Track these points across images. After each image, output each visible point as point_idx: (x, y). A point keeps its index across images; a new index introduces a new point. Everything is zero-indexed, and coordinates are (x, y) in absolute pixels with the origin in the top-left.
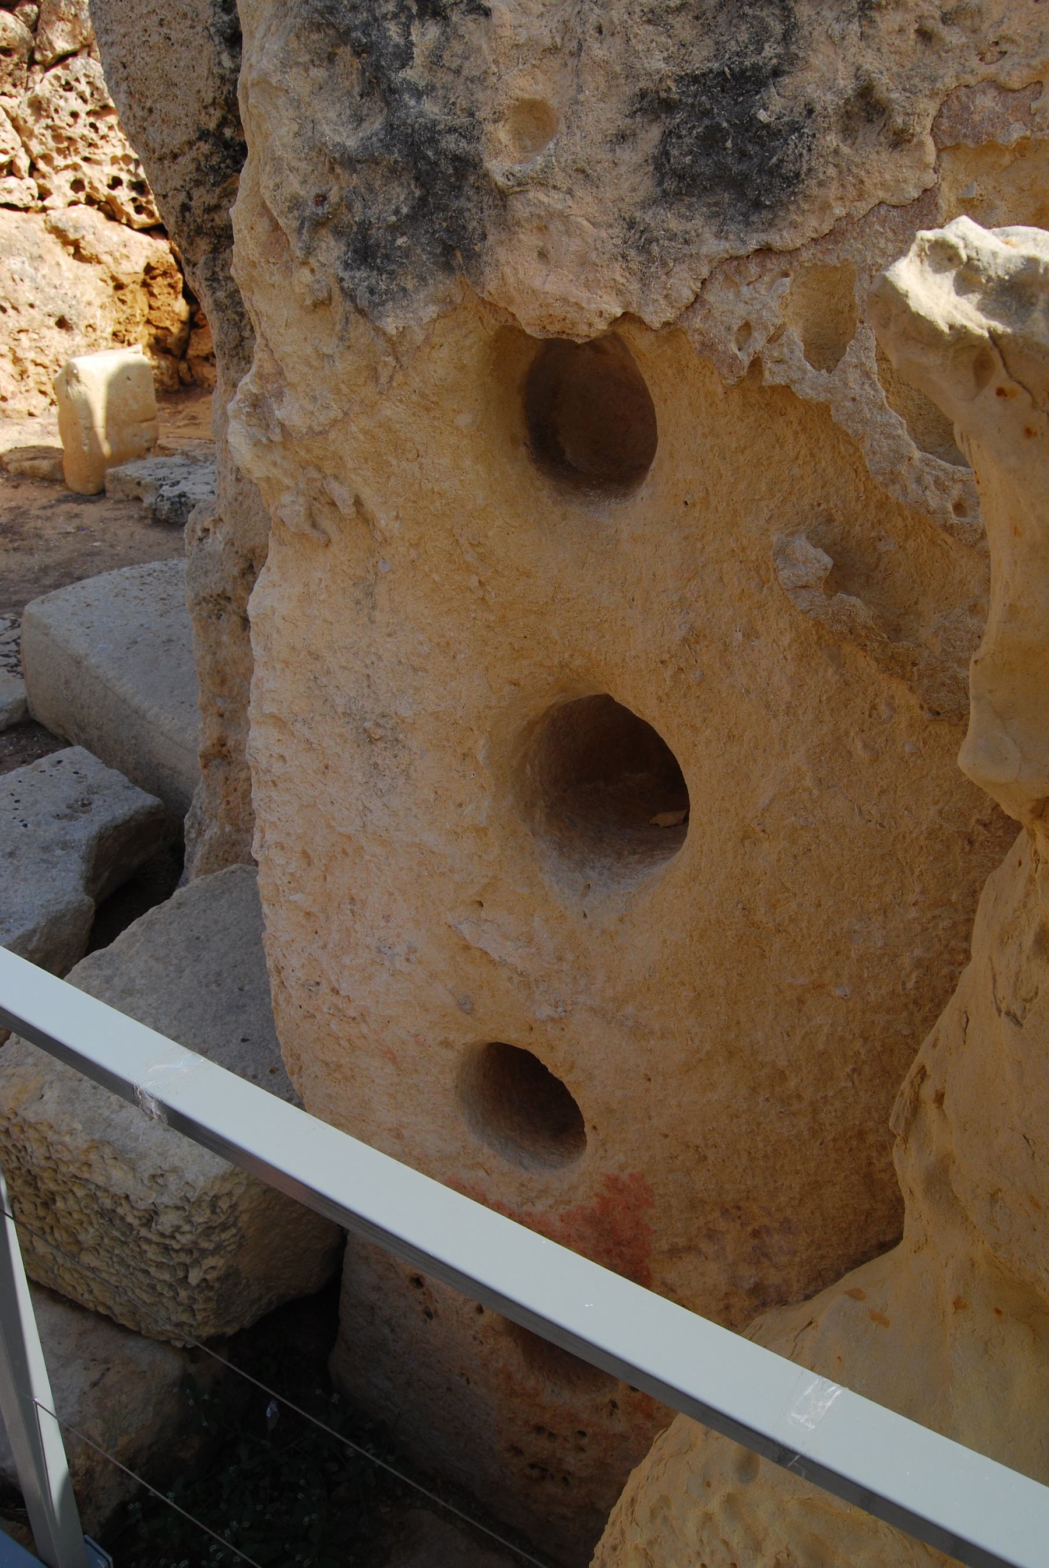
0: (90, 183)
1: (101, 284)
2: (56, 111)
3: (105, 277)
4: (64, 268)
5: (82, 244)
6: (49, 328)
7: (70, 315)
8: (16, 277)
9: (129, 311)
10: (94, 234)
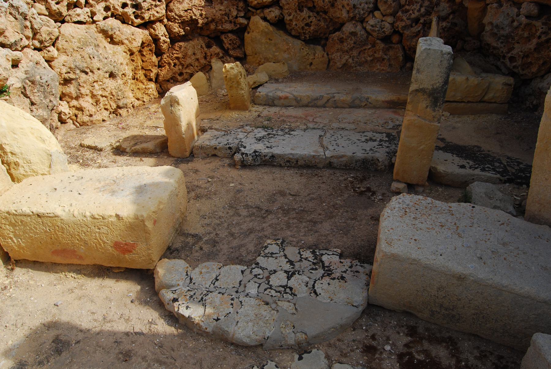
0: (114, 7)
1: (124, 54)
3: (126, 50)
4: (108, 48)
5: (115, 36)
6: (106, 78)
7: (115, 70)
8: (91, 56)
9: (135, 64)
10: (119, 31)
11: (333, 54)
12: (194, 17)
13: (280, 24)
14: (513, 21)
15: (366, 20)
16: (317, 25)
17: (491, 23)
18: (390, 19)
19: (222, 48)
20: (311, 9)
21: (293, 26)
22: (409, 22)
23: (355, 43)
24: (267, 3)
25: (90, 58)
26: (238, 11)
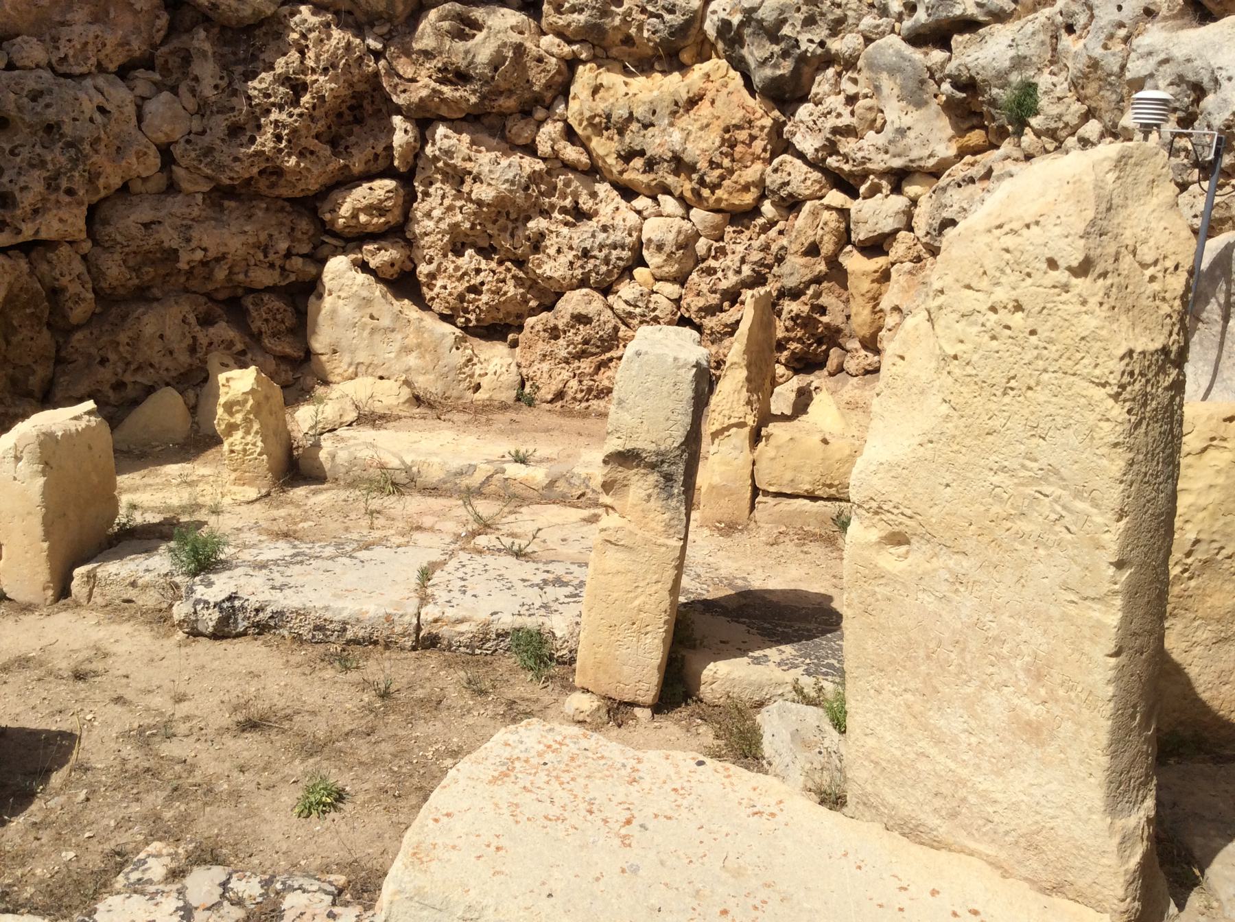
13: (404, 283)
16: (497, 292)
18: (672, 289)
20: (486, 252)
22: (714, 299)
23: (586, 342)
24: (370, 229)
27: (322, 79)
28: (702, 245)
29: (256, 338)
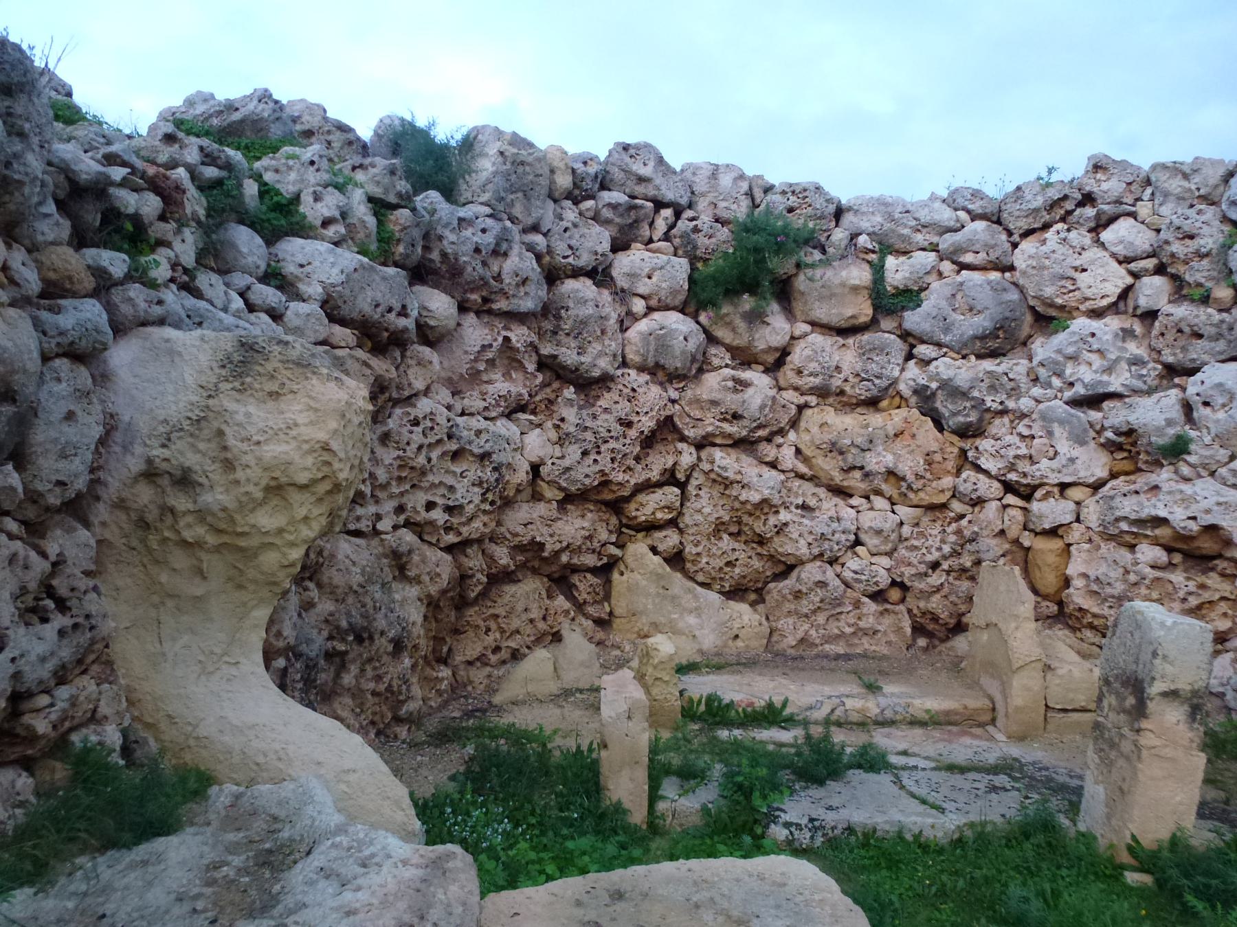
0: (414, 508)
2: (408, 444)
11: (778, 619)
12: (538, 539)
13: (676, 559)
14: (1127, 572)
15: (841, 561)
17: (1085, 576)
18: (885, 561)
19: (571, 597)
20: (735, 535)
21: (701, 566)
22: (922, 568)
23: (822, 601)
25: (375, 608)
26: (611, 532)
27: (643, 419)
28: (906, 530)
29: (580, 607)
